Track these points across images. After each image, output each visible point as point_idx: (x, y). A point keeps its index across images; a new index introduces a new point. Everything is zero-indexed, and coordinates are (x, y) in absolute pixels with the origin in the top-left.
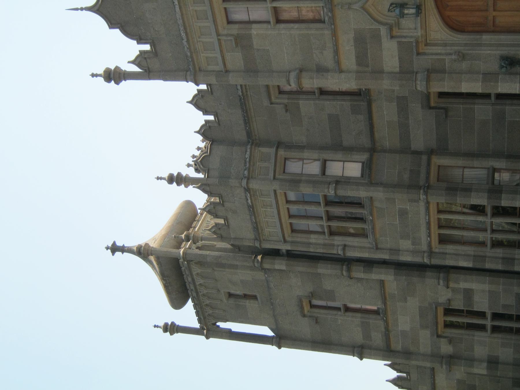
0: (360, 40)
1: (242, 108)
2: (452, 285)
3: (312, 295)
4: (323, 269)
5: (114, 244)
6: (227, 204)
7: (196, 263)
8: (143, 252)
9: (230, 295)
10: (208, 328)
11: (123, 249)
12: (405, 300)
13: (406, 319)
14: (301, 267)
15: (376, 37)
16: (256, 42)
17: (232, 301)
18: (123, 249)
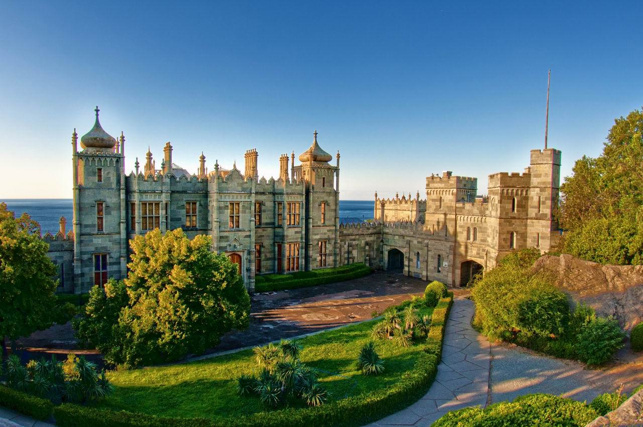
0: (227, 237)
1: (182, 191)
2: (122, 258)
3: (107, 207)
4: (123, 213)
5: (99, 110)
6: (154, 183)
7: (117, 160)
8: (97, 125)
9: (100, 170)
10: (78, 156)
11: (97, 115)
12: (110, 241)
13: (99, 242)
14: (123, 204)
15: (228, 241)
16: (226, 211)
17: (97, 171)
18: (97, 115)
